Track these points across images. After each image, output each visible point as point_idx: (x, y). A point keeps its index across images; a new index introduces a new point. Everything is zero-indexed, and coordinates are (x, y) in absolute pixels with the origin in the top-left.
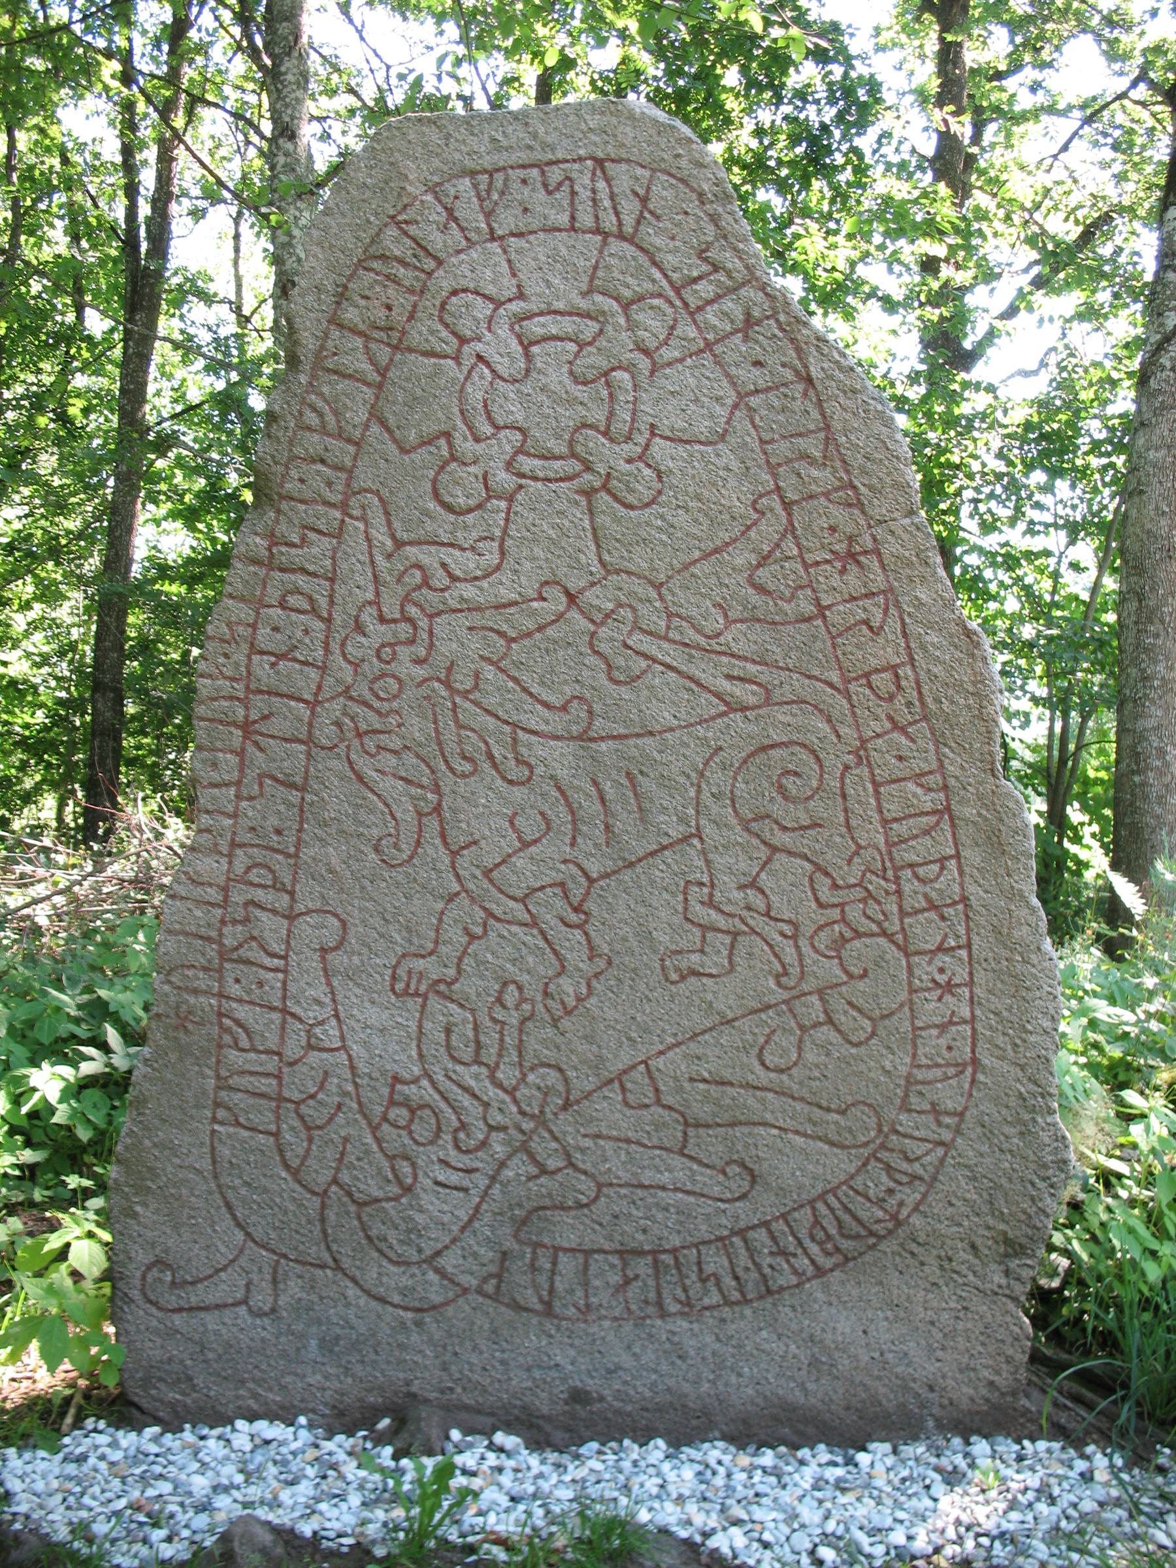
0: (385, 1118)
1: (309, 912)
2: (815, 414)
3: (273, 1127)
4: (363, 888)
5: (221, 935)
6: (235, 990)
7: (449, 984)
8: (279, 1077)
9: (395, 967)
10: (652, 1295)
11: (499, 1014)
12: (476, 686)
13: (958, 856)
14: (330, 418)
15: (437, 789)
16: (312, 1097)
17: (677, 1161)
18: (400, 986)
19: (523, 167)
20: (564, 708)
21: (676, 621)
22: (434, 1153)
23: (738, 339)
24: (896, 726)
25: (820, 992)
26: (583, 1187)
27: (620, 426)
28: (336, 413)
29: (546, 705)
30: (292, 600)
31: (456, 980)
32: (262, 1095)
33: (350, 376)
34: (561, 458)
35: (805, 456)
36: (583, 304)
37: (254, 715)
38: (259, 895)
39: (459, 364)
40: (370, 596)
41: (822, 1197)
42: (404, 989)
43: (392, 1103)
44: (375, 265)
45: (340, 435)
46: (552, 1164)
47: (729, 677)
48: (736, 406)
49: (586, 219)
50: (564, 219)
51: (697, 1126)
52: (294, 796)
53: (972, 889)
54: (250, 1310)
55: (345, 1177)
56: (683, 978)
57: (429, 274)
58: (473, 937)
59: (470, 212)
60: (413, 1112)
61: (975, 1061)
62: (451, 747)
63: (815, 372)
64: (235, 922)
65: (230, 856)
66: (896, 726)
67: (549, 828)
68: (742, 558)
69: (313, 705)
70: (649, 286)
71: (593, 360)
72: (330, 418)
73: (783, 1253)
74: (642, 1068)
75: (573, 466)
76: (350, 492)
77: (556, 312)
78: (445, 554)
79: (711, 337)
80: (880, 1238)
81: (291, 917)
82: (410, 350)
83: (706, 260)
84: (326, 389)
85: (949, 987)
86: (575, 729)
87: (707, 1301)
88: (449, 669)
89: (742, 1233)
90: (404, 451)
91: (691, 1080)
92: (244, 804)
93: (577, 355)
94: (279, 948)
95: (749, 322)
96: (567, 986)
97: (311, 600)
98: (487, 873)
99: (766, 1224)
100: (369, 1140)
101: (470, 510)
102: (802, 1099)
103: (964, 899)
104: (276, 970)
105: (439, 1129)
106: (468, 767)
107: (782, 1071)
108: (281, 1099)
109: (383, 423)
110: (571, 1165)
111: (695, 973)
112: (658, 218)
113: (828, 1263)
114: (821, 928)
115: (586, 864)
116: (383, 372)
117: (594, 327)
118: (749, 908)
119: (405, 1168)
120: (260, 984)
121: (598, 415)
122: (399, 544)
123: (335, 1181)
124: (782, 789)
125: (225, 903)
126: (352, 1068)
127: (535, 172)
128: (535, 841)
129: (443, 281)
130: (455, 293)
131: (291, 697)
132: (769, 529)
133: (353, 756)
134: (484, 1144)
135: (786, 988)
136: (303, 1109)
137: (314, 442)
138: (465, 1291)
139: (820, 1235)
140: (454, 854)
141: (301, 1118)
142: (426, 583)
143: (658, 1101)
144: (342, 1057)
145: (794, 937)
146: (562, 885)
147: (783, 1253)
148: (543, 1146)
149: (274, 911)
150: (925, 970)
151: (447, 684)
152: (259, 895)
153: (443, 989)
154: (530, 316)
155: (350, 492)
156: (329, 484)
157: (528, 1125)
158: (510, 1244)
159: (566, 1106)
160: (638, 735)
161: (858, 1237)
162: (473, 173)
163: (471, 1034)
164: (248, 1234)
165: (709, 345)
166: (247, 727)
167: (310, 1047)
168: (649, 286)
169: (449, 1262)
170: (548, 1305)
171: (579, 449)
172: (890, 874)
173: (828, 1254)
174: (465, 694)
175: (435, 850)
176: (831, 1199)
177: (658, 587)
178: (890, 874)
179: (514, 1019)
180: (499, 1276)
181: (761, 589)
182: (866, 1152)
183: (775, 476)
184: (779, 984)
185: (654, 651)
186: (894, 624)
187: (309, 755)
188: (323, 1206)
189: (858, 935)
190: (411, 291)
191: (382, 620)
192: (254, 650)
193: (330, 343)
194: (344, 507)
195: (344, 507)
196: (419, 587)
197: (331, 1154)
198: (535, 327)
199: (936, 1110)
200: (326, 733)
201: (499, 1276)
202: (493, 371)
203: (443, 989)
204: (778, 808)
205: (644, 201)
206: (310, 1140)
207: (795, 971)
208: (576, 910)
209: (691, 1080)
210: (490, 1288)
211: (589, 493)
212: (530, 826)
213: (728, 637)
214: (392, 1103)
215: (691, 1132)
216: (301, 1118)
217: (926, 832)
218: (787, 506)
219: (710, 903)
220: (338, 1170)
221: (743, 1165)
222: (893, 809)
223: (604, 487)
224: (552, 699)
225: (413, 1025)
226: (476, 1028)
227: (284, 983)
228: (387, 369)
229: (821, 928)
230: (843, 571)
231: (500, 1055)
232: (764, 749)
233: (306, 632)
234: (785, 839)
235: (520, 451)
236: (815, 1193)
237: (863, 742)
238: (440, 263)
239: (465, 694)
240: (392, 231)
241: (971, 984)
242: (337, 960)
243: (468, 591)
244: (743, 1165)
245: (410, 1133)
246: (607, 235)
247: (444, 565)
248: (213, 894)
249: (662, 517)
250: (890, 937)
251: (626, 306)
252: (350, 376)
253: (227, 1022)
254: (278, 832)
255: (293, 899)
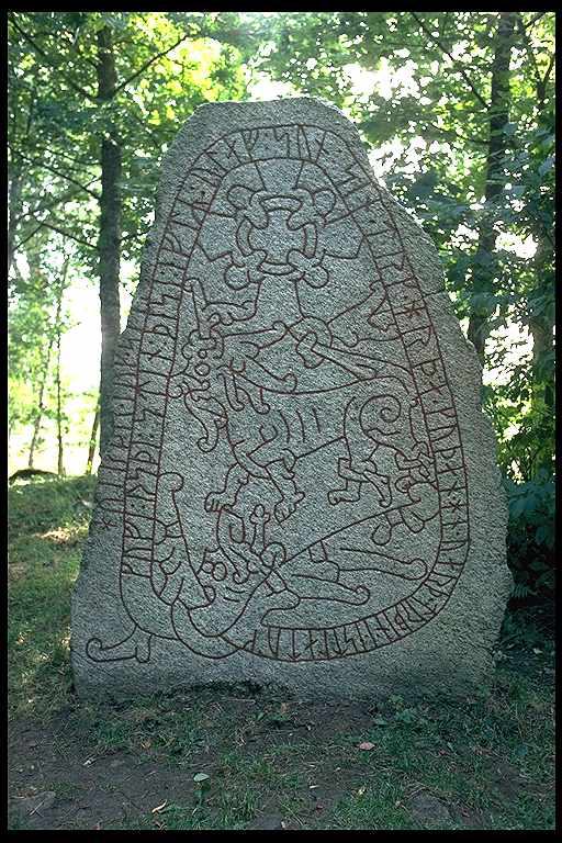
0: (201, 568)
1: (167, 473)
2: (398, 244)
3: (149, 574)
4: (191, 462)
5: (125, 484)
6: (130, 510)
7: (231, 506)
8: (152, 550)
9: (206, 499)
10: (324, 648)
11: (254, 519)
12: (244, 369)
13: (461, 446)
14: (176, 244)
15: (226, 417)
16: (168, 559)
17: (336, 586)
18: (209, 507)
19: (266, 128)
20: (284, 380)
21: (335, 340)
22: (224, 584)
23: (362, 210)
24: (435, 388)
25: (399, 508)
26: (292, 599)
27: (309, 250)
28: (179, 242)
29: (276, 377)
30: (160, 329)
31: (234, 504)
32: (145, 559)
33: (185, 225)
34: (282, 264)
35: (395, 265)
36: (294, 193)
37: (141, 382)
38: (144, 466)
39: (236, 220)
40: (195, 327)
41: (399, 602)
42: (212, 508)
43: (204, 562)
44: (197, 172)
45: (180, 252)
46: (278, 588)
47: (358, 365)
48: (362, 241)
49: (294, 153)
50: (284, 153)
51: (344, 570)
52: (160, 420)
53: (467, 461)
54: (137, 659)
55: (182, 596)
56: (338, 503)
57: (222, 178)
58: (243, 484)
59: (240, 148)
60: (214, 565)
61: (469, 540)
62: (232, 397)
63: (398, 225)
64: (131, 478)
65: (130, 448)
66: (435, 388)
67: (277, 434)
68: (366, 310)
69: (168, 378)
70: (323, 185)
71: (297, 219)
72: (176, 244)
73: (384, 630)
74: (319, 544)
75: (287, 268)
76: (185, 279)
77: (281, 196)
78: (229, 308)
79: (351, 209)
80: (427, 622)
81: (158, 476)
82: (213, 213)
83: (350, 173)
84: (174, 231)
85: (457, 506)
86: (289, 389)
87: (348, 652)
88: (231, 362)
89: (364, 619)
90: (211, 261)
91: (341, 549)
92: (137, 423)
93: (290, 217)
94: (153, 490)
95: (369, 202)
96: (284, 506)
97: (168, 329)
98: (248, 455)
99: (374, 615)
100: (194, 578)
101: (242, 288)
102: (391, 558)
103: (464, 466)
104: (151, 500)
105: (226, 573)
106: (241, 406)
107: (382, 545)
108: (152, 560)
109: (201, 247)
110: (287, 589)
111: (342, 500)
112: (328, 153)
113: (402, 633)
114: (400, 479)
115: (293, 451)
116: (201, 223)
117: (297, 204)
118: (367, 470)
119: (209, 591)
120: (143, 507)
121: (298, 244)
122: (208, 303)
123: (177, 598)
124: (382, 416)
125: (127, 470)
126: (186, 545)
127: (271, 130)
128: (270, 441)
129: (228, 181)
130: (234, 186)
131: (159, 374)
132: (377, 297)
133: (187, 401)
134: (246, 580)
135: (385, 507)
136: (164, 565)
137: (167, 256)
138: (239, 648)
139: (399, 620)
140: (233, 446)
141: (162, 569)
142: (221, 321)
143: (326, 559)
144: (181, 540)
145: (388, 483)
146: (283, 459)
147: (384, 630)
148: (274, 580)
149: (151, 473)
150: (446, 499)
151: (230, 367)
152: (144, 466)
153: (228, 509)
154: (269, 198)
155: (185, 279)
156: (176, 275)
157: (267, 571)
158: (259, 627)
159: (283, 563)
160: (318, 392)
161: (418, 621)
162: (242, 131)
163: (241, 529)
164: (137, 625)
165: (351, 213)
166: (138, 388)
167: (167, 536)
168: (323, 185)
169: (231, 634)
170: (276, 654)
171: (290, 260)
172: (431, 454)
173: (403, 629)
174: (239, 373)
175: (224, 446)
176: (404, 603)
177: (327, 324)
178: (431, 454)
179: (259, 521)
180: (254, 641)
181: (373, 325)
182: (420, 581)
183: (381, 274)
184: (381, 505)
185: (325, 354)
186: (432, 343)
187: (166, 400)
188: (172, 610)
189: (417, 482)
190: (214, 185)
191: (201, 338)
192: (141, 351)
193: (175, 209)
194: (182, 286)
195: (182, 286)
196: (217, 323)
197: (176, 586)
198: (270, 204)
199: (452, 563)
200: (174, 392)
201: (254, 641)
202: (252, 223)
203: (228, 509)
204: (381, 424)
205: (321, 145)
206: (167, 579)
207: (388, 499)
208: (289, 471)
209: (341, 549)
210: (249, 646)
211: (296, 281)
212: (268, 434)
213: (359, 346)
214: (204, 562)
215: (341, 573)
216: (162, 569)
217: (446, 436)
218: (385, 287)
219: (350, 468)
220: (179, 593)
221: (365, 588)
222: (432, 426)
223: (302, 278)
224: (278, 375)
225: (214, 525)
226: (243, 527)
227: (155, 506)
228: (202, 222)
229: (400, 479)
230: (410, 317)
231: (254, 538)
232: (372, 398)
233: (165, 344)
234: (385, 439)
235: (264, 261)
236: (397, 601)
237: (419, 395)
238: (227, 172)
239: (239, 373)
240: (204, 158)
241: (468, 504)
242: (179, 495)
243: (240, 325)
244: (365, 588)
245: (213, 575)
246: (303, 160)
247: (230, 314)
248: (122, 466)
249: (329, 292)
250: (431, 483)
251: (312, 194)
252: (185, 225)
253: (128, 525)
254: (152, 437)
255: (159, 468)
